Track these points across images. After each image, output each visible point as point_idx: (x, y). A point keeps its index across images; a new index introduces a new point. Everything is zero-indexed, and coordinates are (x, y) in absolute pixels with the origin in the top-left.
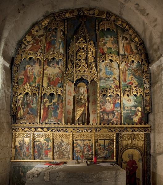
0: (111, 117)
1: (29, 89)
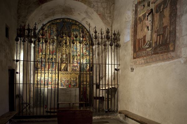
0: (76, 68)
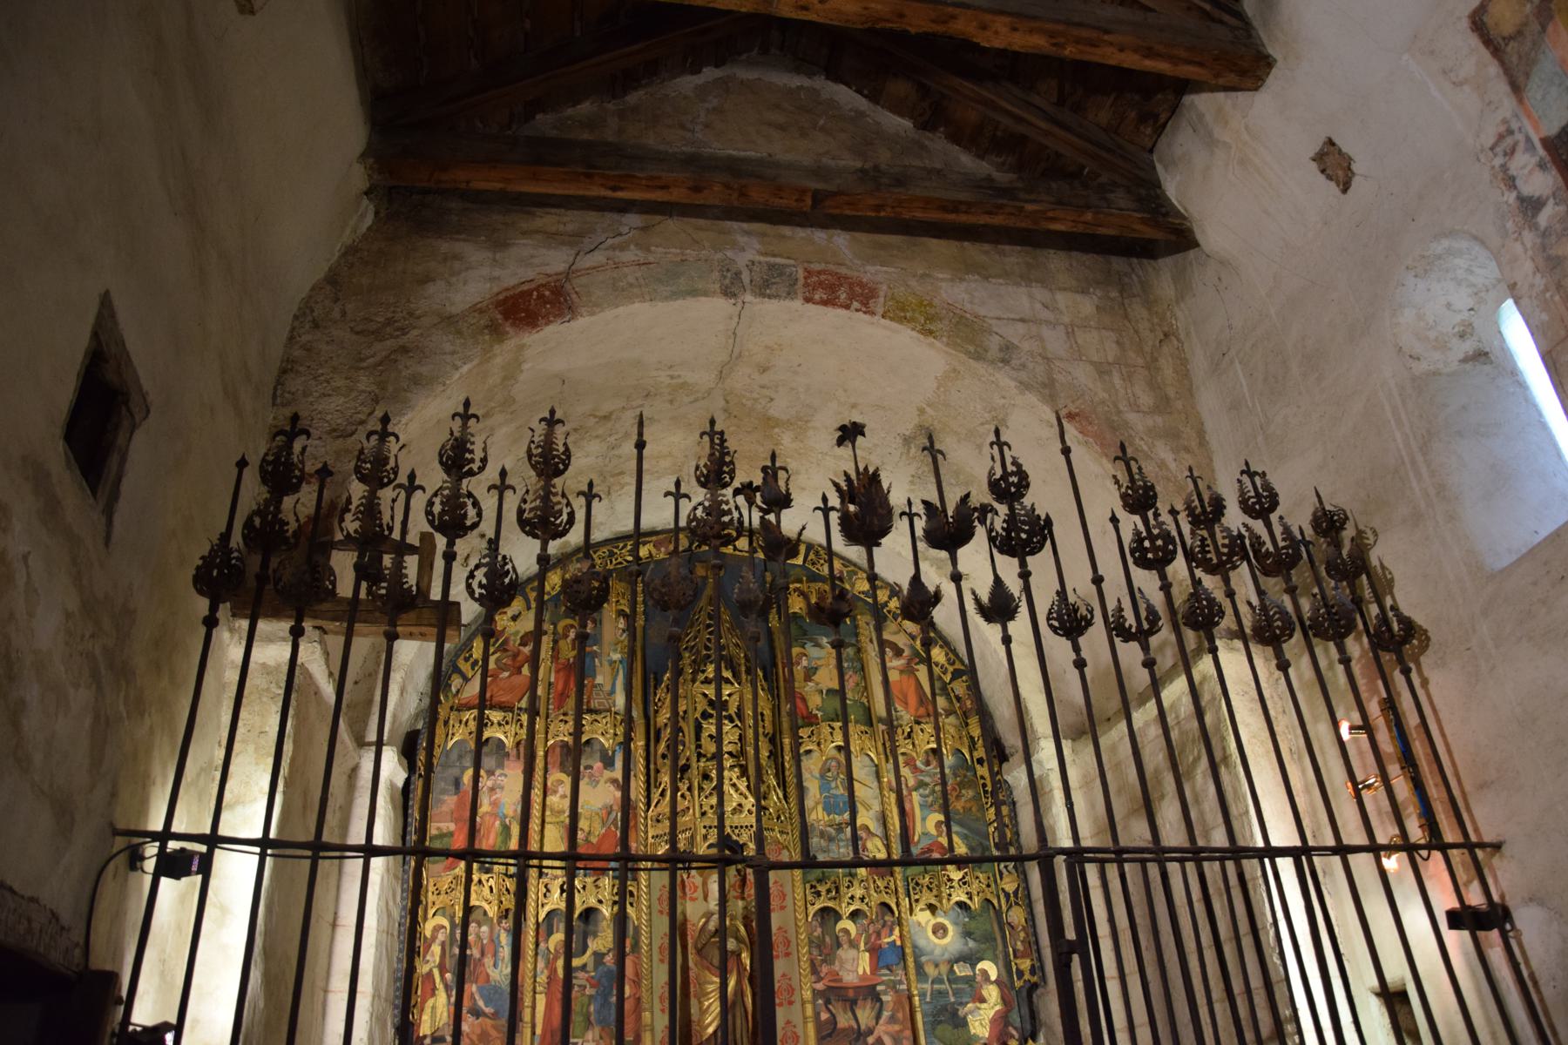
1: (486, 891)
